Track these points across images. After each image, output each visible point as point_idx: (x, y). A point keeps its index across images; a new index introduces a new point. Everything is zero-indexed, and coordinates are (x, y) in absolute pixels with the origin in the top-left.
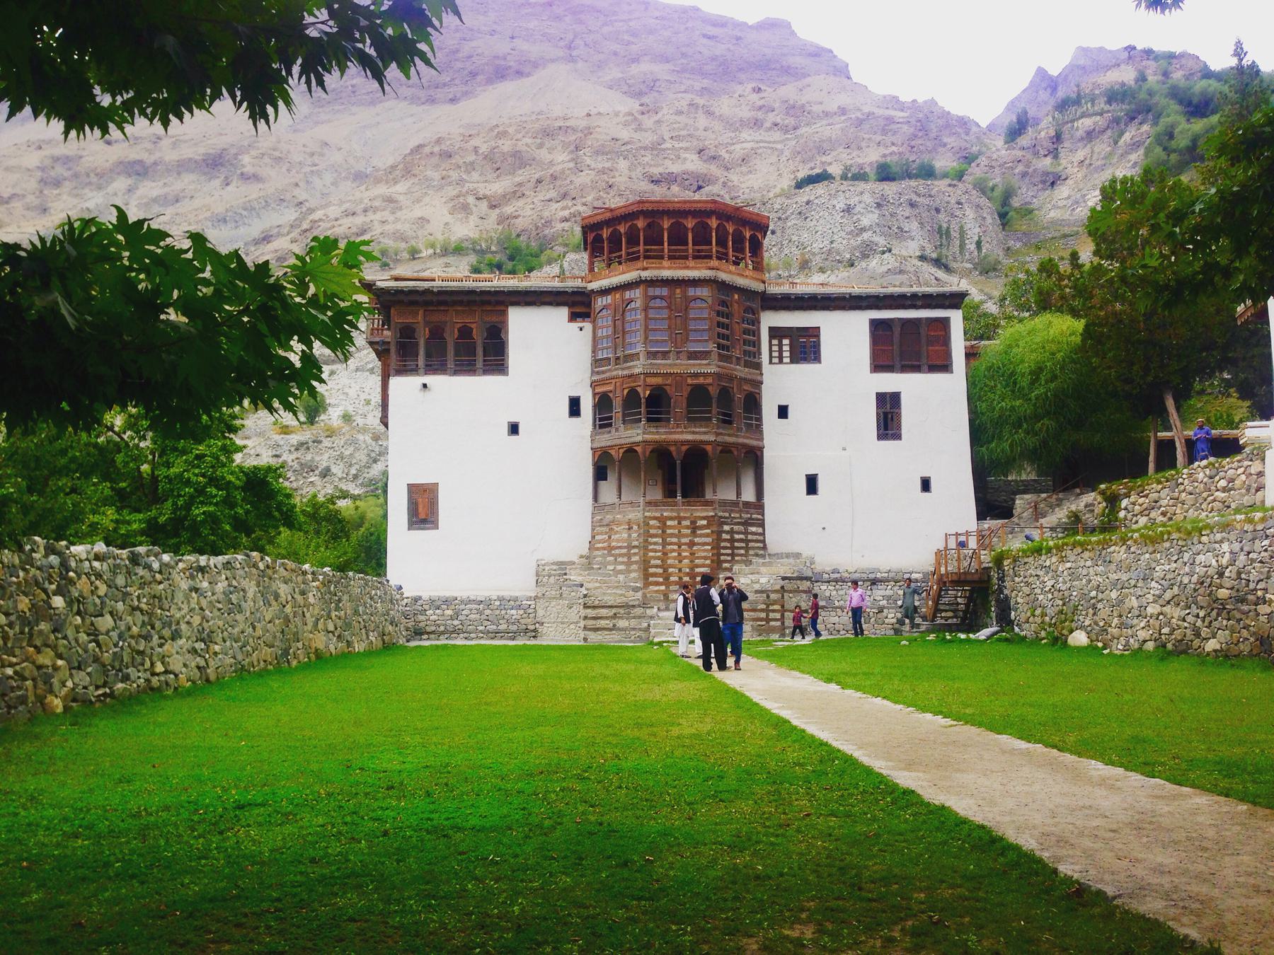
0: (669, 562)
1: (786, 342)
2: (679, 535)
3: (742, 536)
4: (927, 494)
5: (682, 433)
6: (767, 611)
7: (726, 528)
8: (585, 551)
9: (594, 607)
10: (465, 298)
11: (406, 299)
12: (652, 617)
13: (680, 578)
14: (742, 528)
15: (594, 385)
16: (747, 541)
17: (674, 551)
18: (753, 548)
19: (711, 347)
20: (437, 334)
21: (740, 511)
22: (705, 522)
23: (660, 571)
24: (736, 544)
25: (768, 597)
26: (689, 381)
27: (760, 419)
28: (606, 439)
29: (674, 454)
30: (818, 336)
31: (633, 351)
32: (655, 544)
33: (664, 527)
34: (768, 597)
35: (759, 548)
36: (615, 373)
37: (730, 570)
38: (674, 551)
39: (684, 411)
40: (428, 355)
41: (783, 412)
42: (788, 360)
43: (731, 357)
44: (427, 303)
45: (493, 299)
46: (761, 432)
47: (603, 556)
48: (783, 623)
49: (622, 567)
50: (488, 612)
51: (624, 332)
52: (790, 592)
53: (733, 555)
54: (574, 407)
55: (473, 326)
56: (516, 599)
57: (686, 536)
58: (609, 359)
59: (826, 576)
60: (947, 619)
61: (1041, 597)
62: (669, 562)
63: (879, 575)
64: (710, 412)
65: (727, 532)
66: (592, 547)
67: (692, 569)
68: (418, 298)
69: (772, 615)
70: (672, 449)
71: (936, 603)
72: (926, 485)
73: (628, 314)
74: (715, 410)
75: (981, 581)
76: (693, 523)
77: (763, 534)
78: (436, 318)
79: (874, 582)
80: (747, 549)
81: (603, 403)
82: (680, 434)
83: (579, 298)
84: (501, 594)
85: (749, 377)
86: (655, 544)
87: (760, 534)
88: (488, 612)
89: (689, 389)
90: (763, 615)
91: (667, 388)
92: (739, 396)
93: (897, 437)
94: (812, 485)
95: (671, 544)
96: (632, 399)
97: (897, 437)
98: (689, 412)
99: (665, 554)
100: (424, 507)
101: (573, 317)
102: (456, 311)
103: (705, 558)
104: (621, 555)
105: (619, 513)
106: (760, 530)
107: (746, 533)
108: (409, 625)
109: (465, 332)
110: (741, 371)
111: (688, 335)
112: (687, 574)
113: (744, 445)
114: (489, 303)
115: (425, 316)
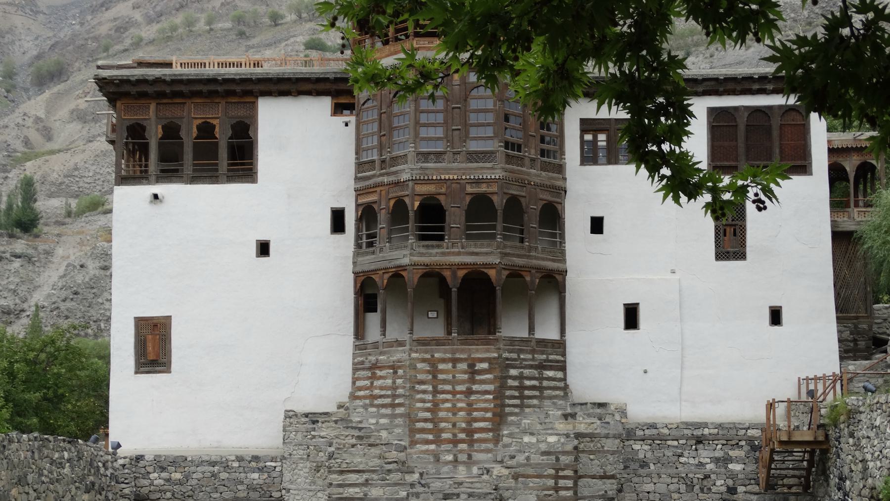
0: (442, 414)
1: (602, 137)
2: (454, 382)
3: (535, 383)
4: (776, 327)
5: (459, 254)
6: (557, 477)
7: (513, 372)
8: (345, 399)
9: (342, 472)
10: (205, 88)
11: (133, 90)
12: (412, 485)
13: (455, 435)
14: (535, 373)
15: (359, 193)
16: (540, 389)
17: (447, 401)
18: (550, 398)
19: (494, 145)
20: (171, 132)
21: (533, 352)
22: (485, 365)
23: (430, 426)
24: (527, 393)
25: (557, 459)
26: (469, 189)
27: (562, 236)
28: (369, 262)
29: (449, 280)
31: (401, 153)
32: (424, 392)
33: (434, 372)
34: (557, 459)
35: (556, 397)
36: (380, 179)
37: (518, 425)
38: (447, 401)
39: (463, 228)
40: (163, 158)
41: (597, 225)
42: (604, 160)
43: (522, 159)
44: (160, 95)
45: (238, 89)
46: (563, 253)
47: (365, 407)
48: (576, 493)
49: (383, 421)
50: (224, 475)
51: (392, 129)
52: (591, 452)
53: (521, 406)
54: (338, 222)
55: (215, 122)
56: (256, 458)
57: (462, 382)
58: (373, 162)
59: (639, 433)
60: (790, 487)
61: (871, 464)
62: (442, 414)
63: (706, 431)
64: (494, 227)
65: (514, 378)
66: (353, 397)
67: (469, 423)
68: (150, 89)
69: (562, 483)
70: (447, 274)
71: (770, 469)
72: (776, 317)
73: (395, 106)
74: (500, 225)
75: (815, 442)
76: (472, 366)
77: (565, 379)
78: (172, 113)
79: (699, 441)
81: (367, 215)
82: (456, 254)
83: (342, 86)
84: (239, 454)
86: (424, 392)
87: (560, 380)
88: (224, 475)
89: (468, 199)
90: (551, 482)
91: (442, 198)
92: (533, 209)
93: (741, 255)
94: (631, 317)
95: (443, 392)
96: (399, 211)
97: (741, 255)
98: (468, 228)
99: (436, 404)
100: (154, 346)
101: (338, 109)
102: (196, 104)
103: (486, 410)
104: (384, 406)
105: (381, 353)
106: (560, 375)
107: (541, 379)
108: (127, 491)
109: (206, 130)
110: (535, 175)
111: (467, 133)
112: (463, 430)
113: (539, 269)
114: (232, 93)
115: (157, 110)
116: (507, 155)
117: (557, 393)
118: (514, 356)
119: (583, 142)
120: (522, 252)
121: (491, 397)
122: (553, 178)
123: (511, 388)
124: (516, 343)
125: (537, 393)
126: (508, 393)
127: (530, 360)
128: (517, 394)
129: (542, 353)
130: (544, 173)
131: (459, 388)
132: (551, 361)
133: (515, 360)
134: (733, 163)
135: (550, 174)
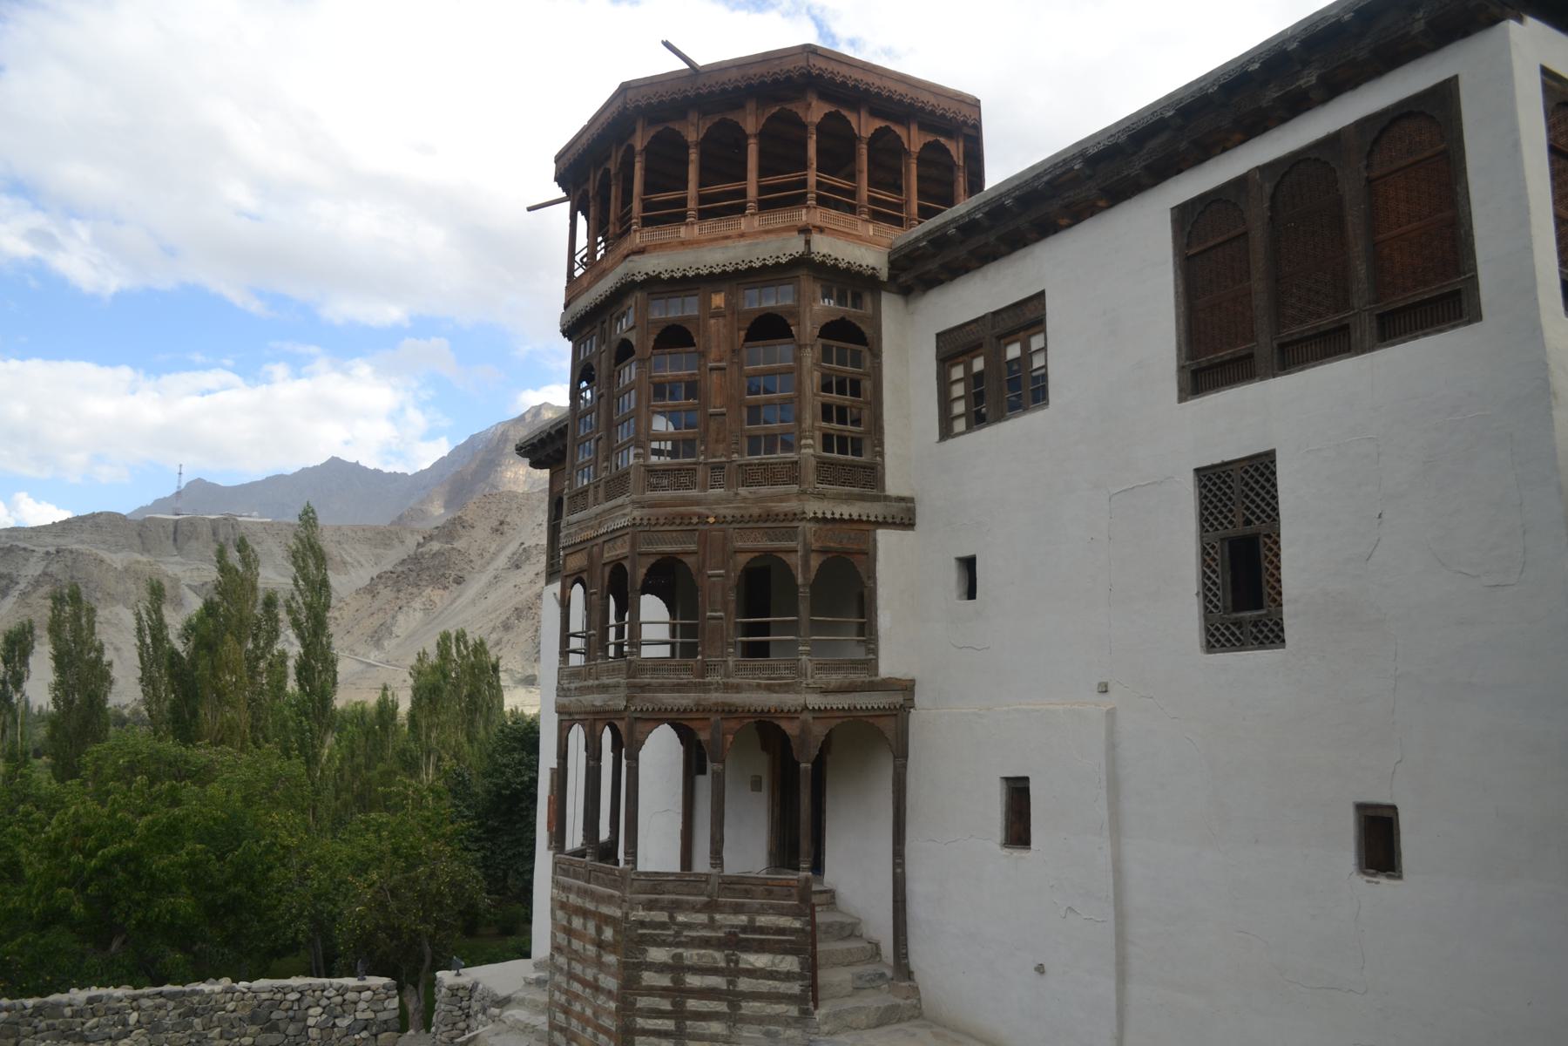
1: (978, 364)
7: (657, 954)
14: (719, 957)
16: (733, 998)
18: (760, 1020)
21: (711, 907)
24: (692, 1004)
30: (1038, 324)
33: (569, 932)
65: (661, 968)
76: (599, 931)
80: (733, 1018)
85: (756, 511)
87: (788, 976)
89: (607, 570)
106: (790, 963)
113: (729, 712)
116: (651, 471)
117: (780, 1008)
118: (662, 917)
119: (944, 384)
120: (686, 678)
121: (612, 1005)
122: (772, 498)
123: (651, 991)
124: (669, 886)
125: (722, 1007)
126: (643, 1002)
127: (704, 926)
128: (666, 1005)
129: (737, 909)
130: (743, 491)
131: (589, 974)
132: (761, 930)
133: (663, 926)
134: (1242, 349)
135: (765, 490)
